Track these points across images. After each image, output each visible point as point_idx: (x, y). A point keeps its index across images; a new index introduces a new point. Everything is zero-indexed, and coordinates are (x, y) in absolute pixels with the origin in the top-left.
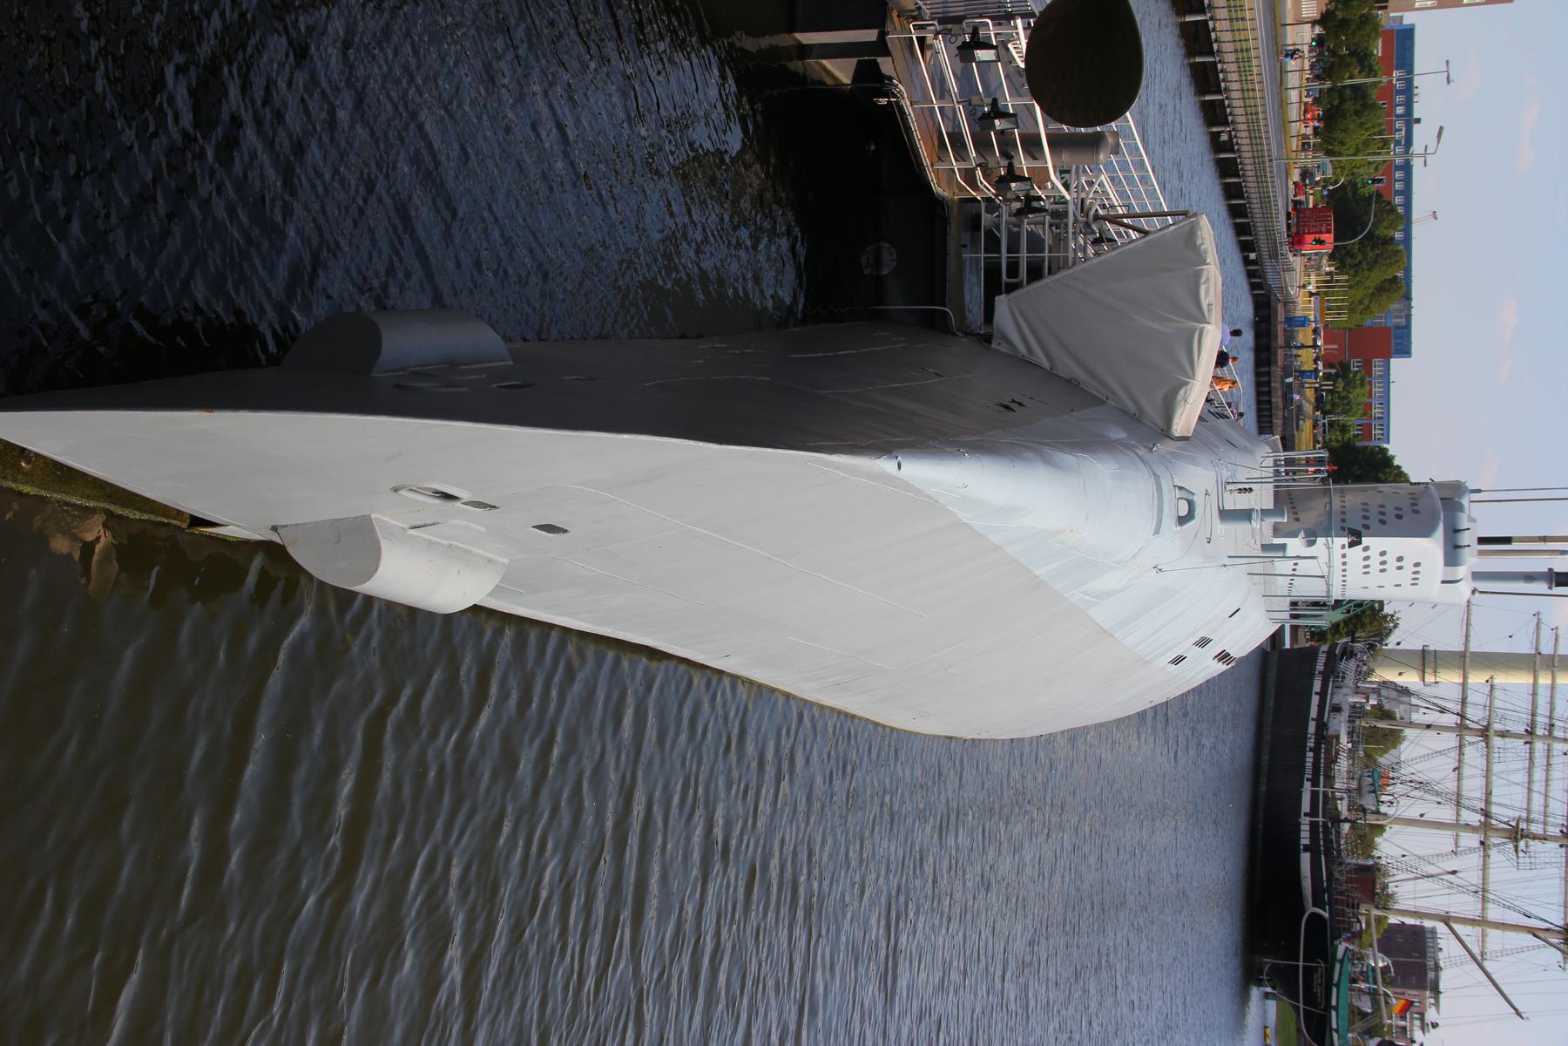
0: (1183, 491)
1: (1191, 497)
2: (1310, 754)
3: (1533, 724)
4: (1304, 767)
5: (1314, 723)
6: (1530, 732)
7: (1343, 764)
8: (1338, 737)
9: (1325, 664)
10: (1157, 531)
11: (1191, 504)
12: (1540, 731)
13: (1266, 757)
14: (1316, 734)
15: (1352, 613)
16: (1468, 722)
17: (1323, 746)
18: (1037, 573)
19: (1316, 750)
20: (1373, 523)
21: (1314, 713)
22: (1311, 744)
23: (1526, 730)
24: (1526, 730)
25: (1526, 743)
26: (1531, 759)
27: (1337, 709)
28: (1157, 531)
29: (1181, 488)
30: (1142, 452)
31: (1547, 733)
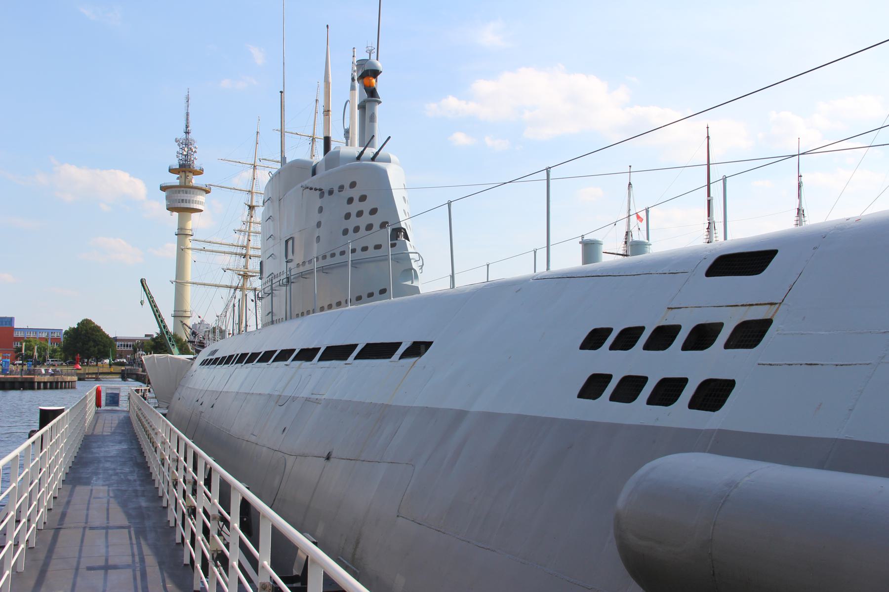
3: (241, 255)
6: (245, 256)
12: (244, 252)
15: (174, 343)
16: (240, 285)
23: (243, 258)
24: (243, 258)
25: (250, 258)
31: (245, 248)
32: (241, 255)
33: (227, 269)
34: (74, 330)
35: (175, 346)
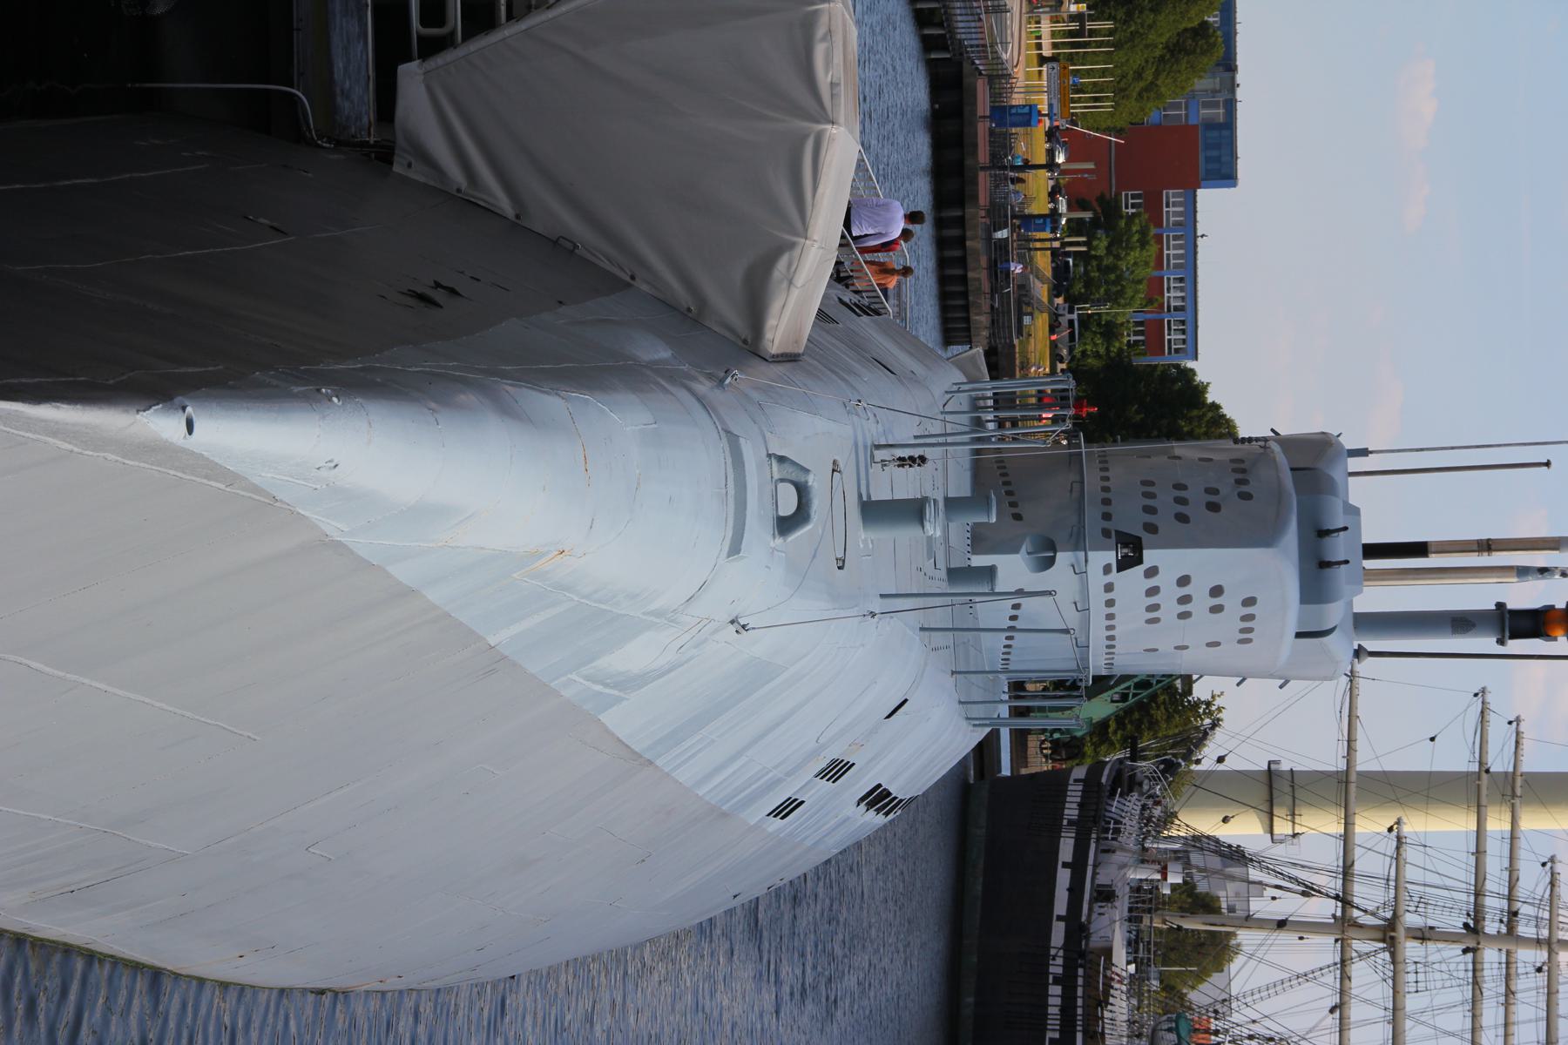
0: (786, 465)
1: (801, 478)
2: (1055, 990)
3: (1478, 913)
4: (1045, 1015)
5: (1062, 925)
6: (1474, 929)
7: (1120, 1007)
8: (1108, 952)
9: (1081, 805)
10: (735, 549)
11: (802, 491)
12: (1491, 927)
13: (971, 1000)
14: (1065, 947)
15: (1131, 701)
16: (1356, 913)
17: (1080, 971)
18: (492, 641)
19: (1067, 981)
20: (1164, 520)
21: (1061, 906)
22: (1056, 968)
24: (1466, 925)
25: (1465, 951)
26: (1476, 983)
27: (1105, 895)
28: (735, 549)
29: (782, 459)
30: (703, 387)
31: (1504, 930)
32: (1478, 913)
33: (1399, 838)
34: (1199, 391)
35: (1121, 705)
